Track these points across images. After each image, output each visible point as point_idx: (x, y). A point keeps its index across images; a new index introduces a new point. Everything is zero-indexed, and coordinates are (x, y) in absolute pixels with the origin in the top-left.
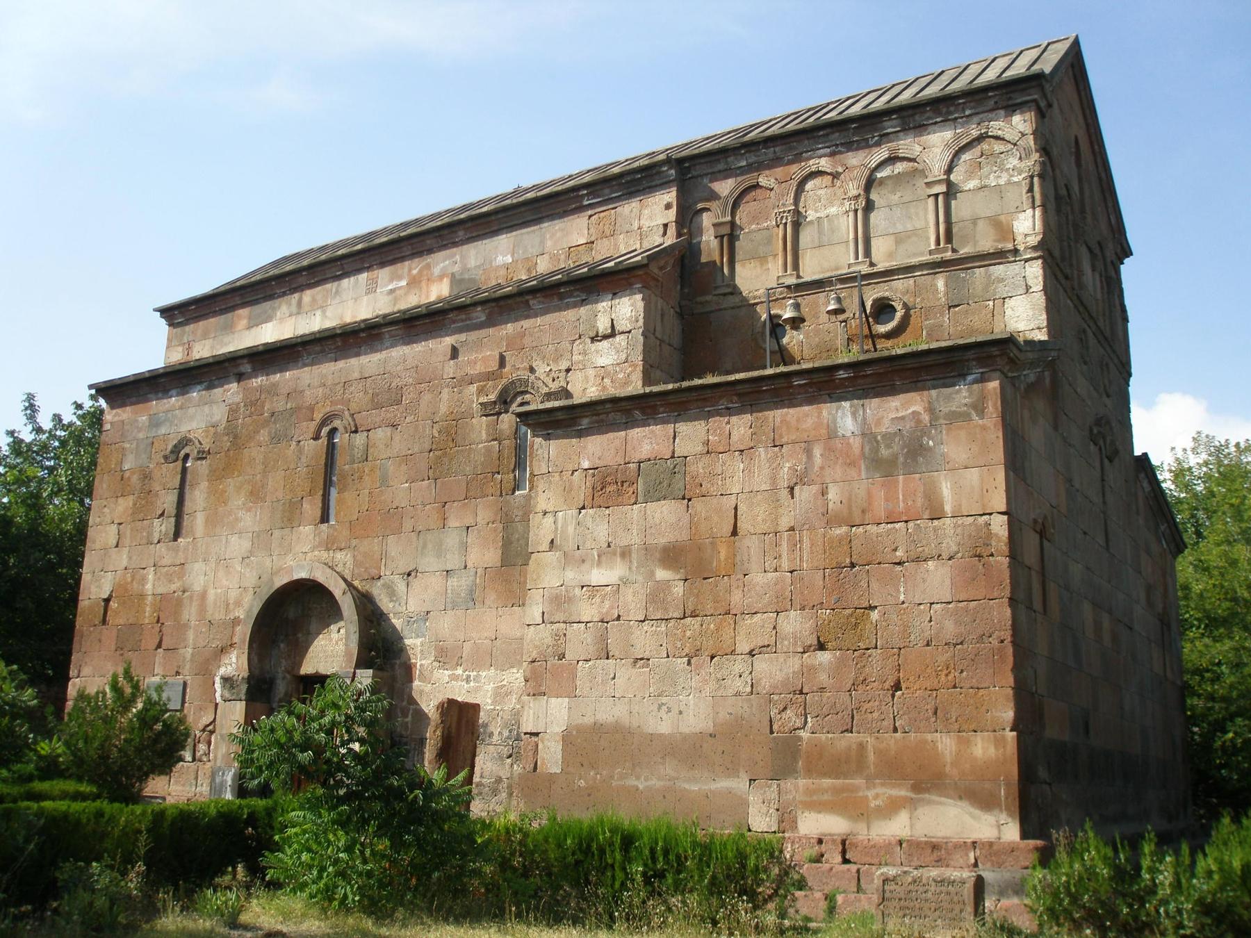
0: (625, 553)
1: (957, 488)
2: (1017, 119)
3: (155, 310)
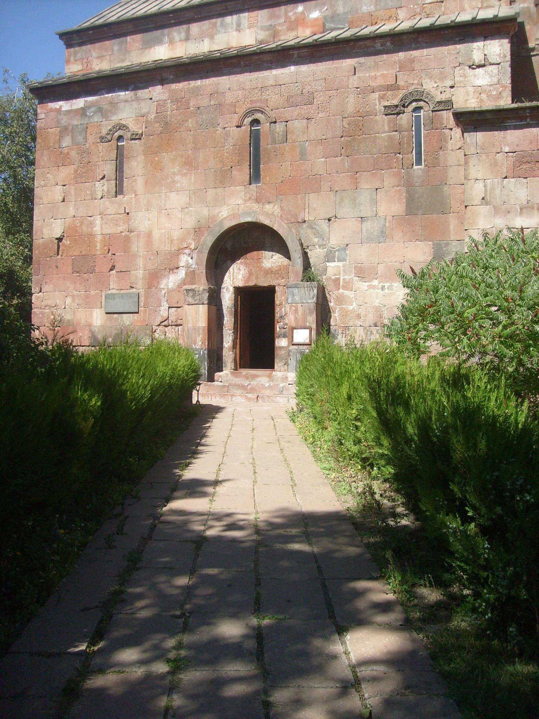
3: (57, 34)
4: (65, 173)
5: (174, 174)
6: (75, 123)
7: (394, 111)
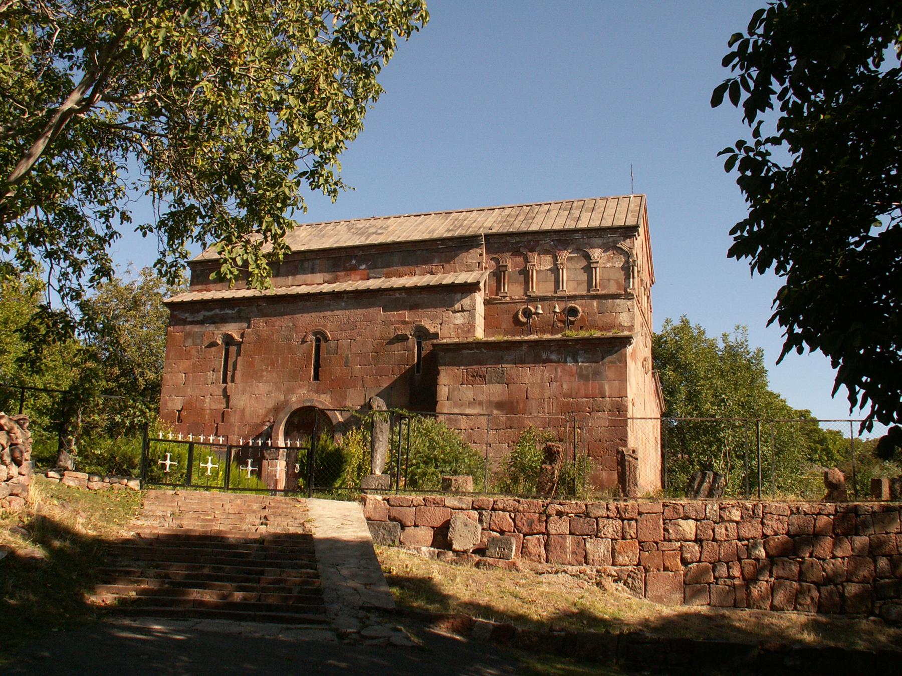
0: (480, 403)
1: (611, 388)
4: (185, 364)
5: (263, 371)
6: (196, 330)
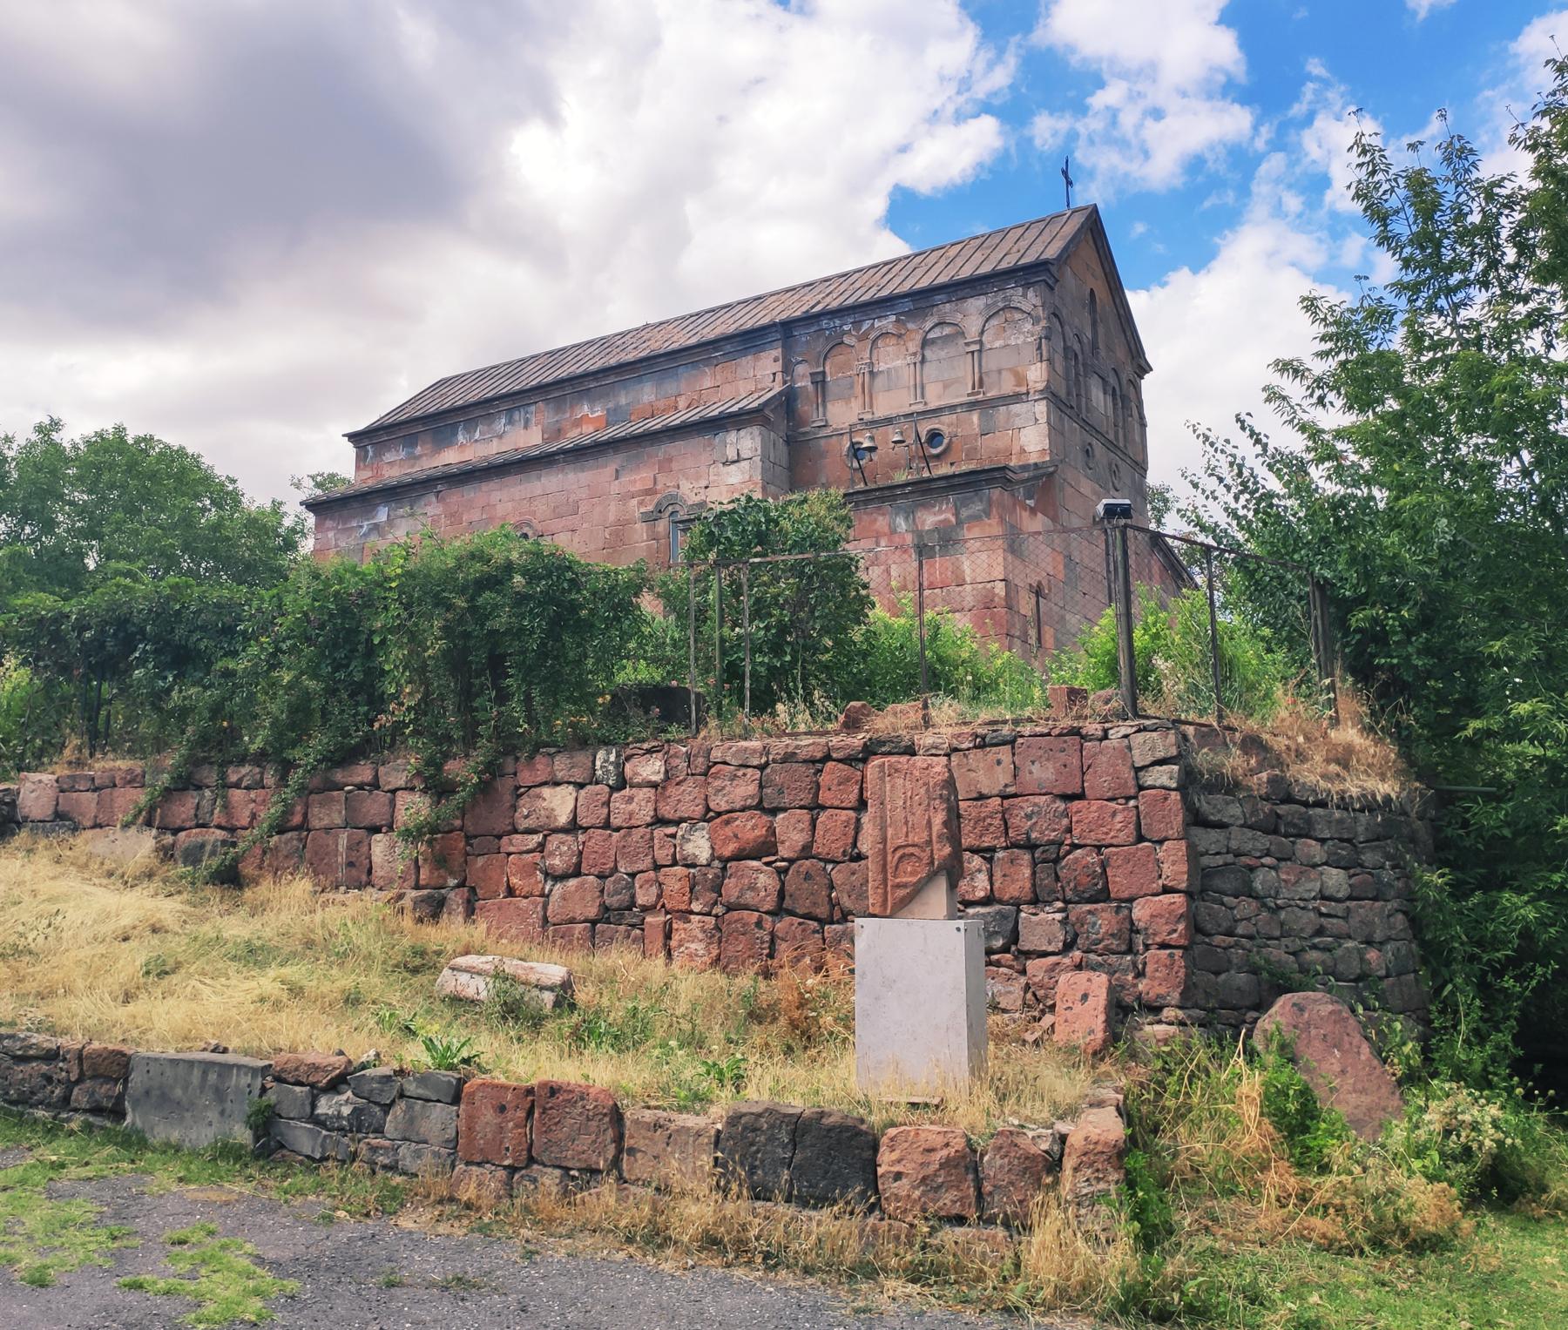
2: (1031, 293)
7: (651, 519)
